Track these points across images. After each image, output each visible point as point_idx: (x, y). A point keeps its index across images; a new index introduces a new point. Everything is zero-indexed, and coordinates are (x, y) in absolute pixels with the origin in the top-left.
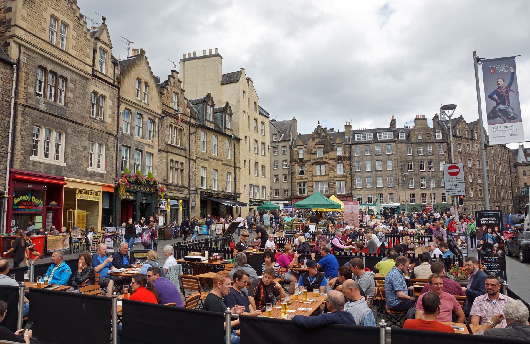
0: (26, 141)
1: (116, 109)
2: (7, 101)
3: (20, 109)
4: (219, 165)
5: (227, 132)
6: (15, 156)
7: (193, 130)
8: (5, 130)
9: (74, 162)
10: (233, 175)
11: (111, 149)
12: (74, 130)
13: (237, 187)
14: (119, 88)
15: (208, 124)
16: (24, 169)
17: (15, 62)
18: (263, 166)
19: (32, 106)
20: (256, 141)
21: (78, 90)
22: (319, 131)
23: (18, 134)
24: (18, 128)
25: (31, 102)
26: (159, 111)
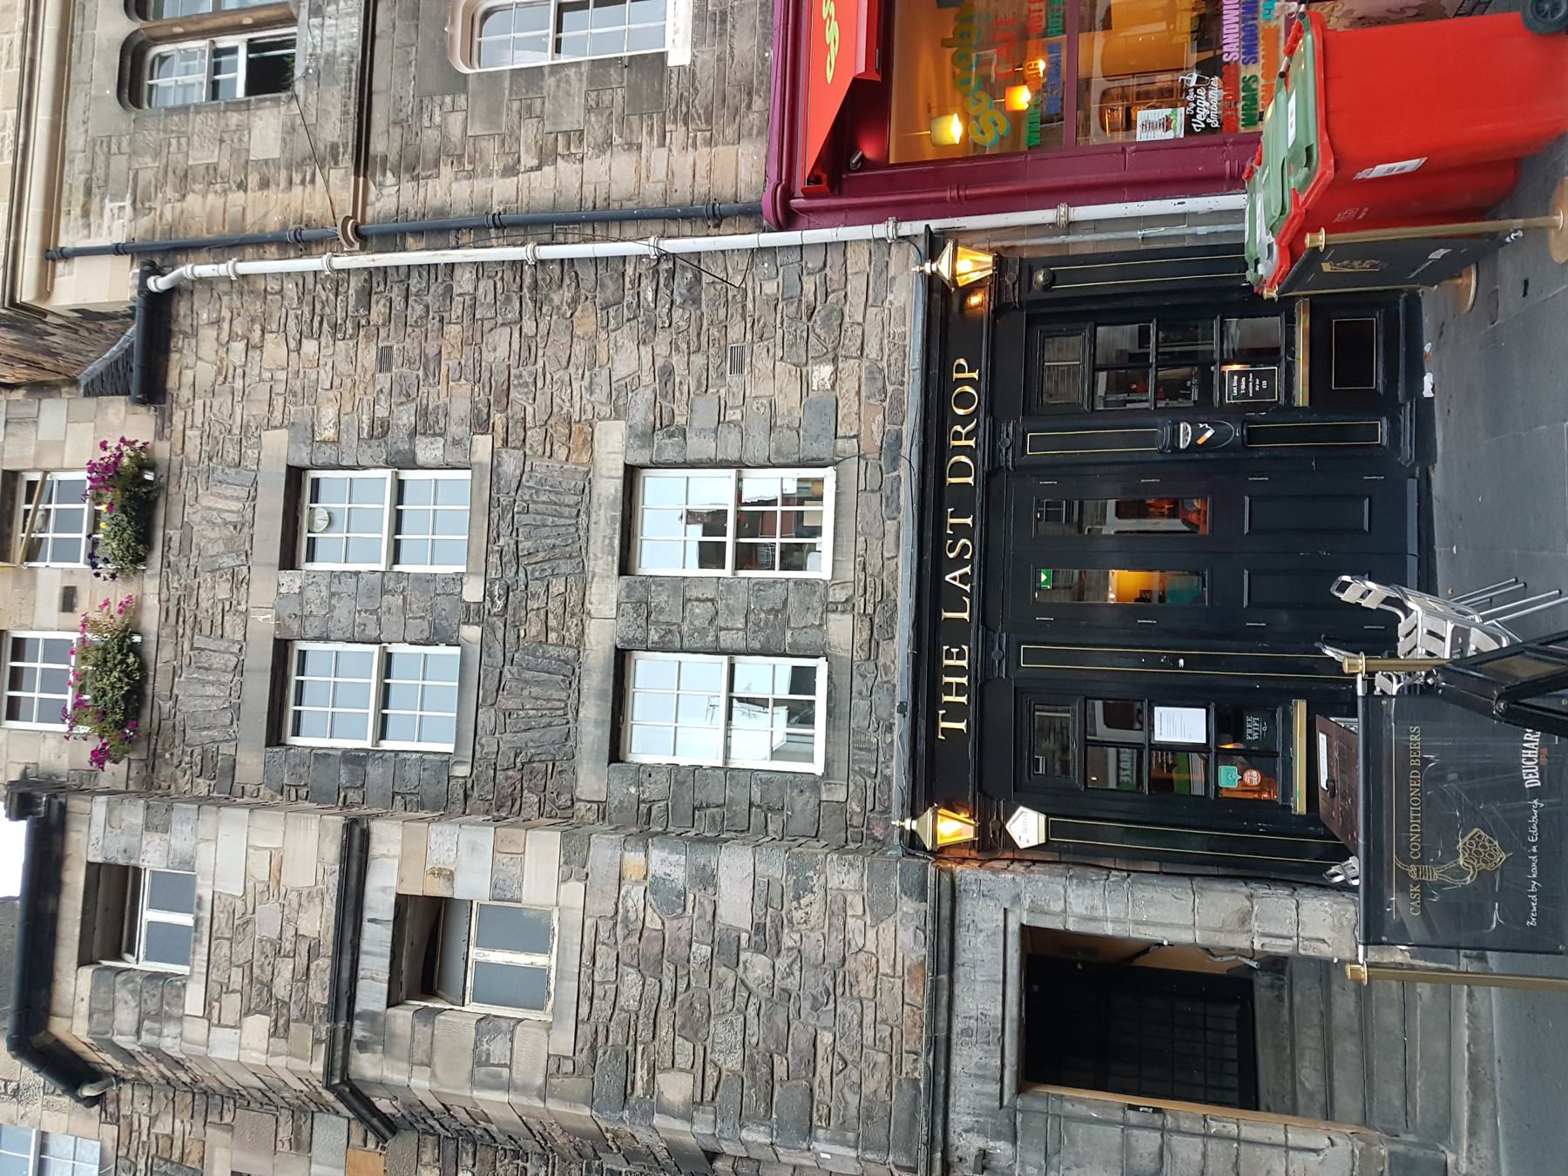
0: (573, 118)
2: (366, 296)
3: (389, 197)
6: (682, 192)
8: (535, 286)
16: (758, 103)
19: (352, 109)
23: (544, 186)
24: (501, 192)
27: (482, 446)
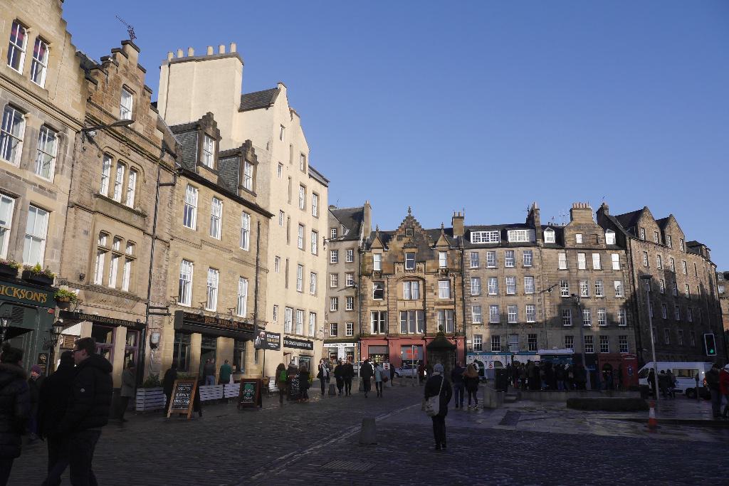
5: (245, 196)
7: (167, 177)
13: (259, 309)
15: (202, 173)
22: (410, 226)
26: (79, 115)
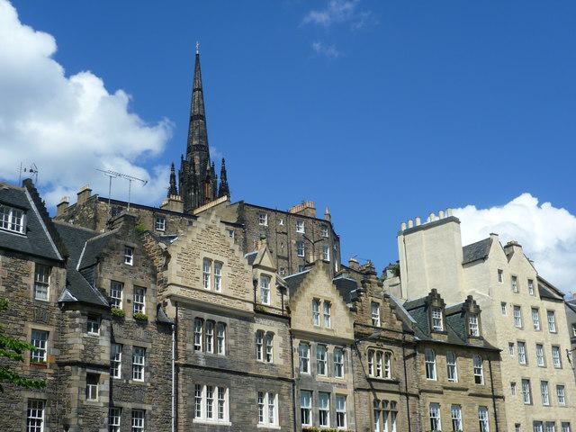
1: (289, 345)
4: (461, 397)
7: (409, 351)
9: (241, 420)
10: (491, 410)
11: (286, 397)
12: (237, 382)
14: (290, 319)
17: (173, 321)
18: (560, 387)
20: (540, 346)
21: (239, 334)
25: (190, 361)
26: (350, 336)
27: (149, 384)
